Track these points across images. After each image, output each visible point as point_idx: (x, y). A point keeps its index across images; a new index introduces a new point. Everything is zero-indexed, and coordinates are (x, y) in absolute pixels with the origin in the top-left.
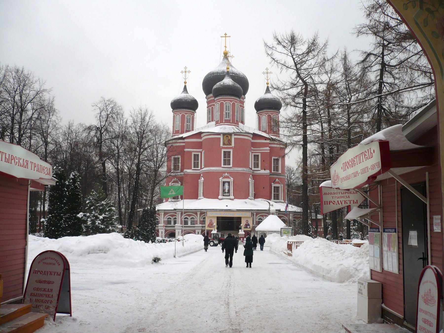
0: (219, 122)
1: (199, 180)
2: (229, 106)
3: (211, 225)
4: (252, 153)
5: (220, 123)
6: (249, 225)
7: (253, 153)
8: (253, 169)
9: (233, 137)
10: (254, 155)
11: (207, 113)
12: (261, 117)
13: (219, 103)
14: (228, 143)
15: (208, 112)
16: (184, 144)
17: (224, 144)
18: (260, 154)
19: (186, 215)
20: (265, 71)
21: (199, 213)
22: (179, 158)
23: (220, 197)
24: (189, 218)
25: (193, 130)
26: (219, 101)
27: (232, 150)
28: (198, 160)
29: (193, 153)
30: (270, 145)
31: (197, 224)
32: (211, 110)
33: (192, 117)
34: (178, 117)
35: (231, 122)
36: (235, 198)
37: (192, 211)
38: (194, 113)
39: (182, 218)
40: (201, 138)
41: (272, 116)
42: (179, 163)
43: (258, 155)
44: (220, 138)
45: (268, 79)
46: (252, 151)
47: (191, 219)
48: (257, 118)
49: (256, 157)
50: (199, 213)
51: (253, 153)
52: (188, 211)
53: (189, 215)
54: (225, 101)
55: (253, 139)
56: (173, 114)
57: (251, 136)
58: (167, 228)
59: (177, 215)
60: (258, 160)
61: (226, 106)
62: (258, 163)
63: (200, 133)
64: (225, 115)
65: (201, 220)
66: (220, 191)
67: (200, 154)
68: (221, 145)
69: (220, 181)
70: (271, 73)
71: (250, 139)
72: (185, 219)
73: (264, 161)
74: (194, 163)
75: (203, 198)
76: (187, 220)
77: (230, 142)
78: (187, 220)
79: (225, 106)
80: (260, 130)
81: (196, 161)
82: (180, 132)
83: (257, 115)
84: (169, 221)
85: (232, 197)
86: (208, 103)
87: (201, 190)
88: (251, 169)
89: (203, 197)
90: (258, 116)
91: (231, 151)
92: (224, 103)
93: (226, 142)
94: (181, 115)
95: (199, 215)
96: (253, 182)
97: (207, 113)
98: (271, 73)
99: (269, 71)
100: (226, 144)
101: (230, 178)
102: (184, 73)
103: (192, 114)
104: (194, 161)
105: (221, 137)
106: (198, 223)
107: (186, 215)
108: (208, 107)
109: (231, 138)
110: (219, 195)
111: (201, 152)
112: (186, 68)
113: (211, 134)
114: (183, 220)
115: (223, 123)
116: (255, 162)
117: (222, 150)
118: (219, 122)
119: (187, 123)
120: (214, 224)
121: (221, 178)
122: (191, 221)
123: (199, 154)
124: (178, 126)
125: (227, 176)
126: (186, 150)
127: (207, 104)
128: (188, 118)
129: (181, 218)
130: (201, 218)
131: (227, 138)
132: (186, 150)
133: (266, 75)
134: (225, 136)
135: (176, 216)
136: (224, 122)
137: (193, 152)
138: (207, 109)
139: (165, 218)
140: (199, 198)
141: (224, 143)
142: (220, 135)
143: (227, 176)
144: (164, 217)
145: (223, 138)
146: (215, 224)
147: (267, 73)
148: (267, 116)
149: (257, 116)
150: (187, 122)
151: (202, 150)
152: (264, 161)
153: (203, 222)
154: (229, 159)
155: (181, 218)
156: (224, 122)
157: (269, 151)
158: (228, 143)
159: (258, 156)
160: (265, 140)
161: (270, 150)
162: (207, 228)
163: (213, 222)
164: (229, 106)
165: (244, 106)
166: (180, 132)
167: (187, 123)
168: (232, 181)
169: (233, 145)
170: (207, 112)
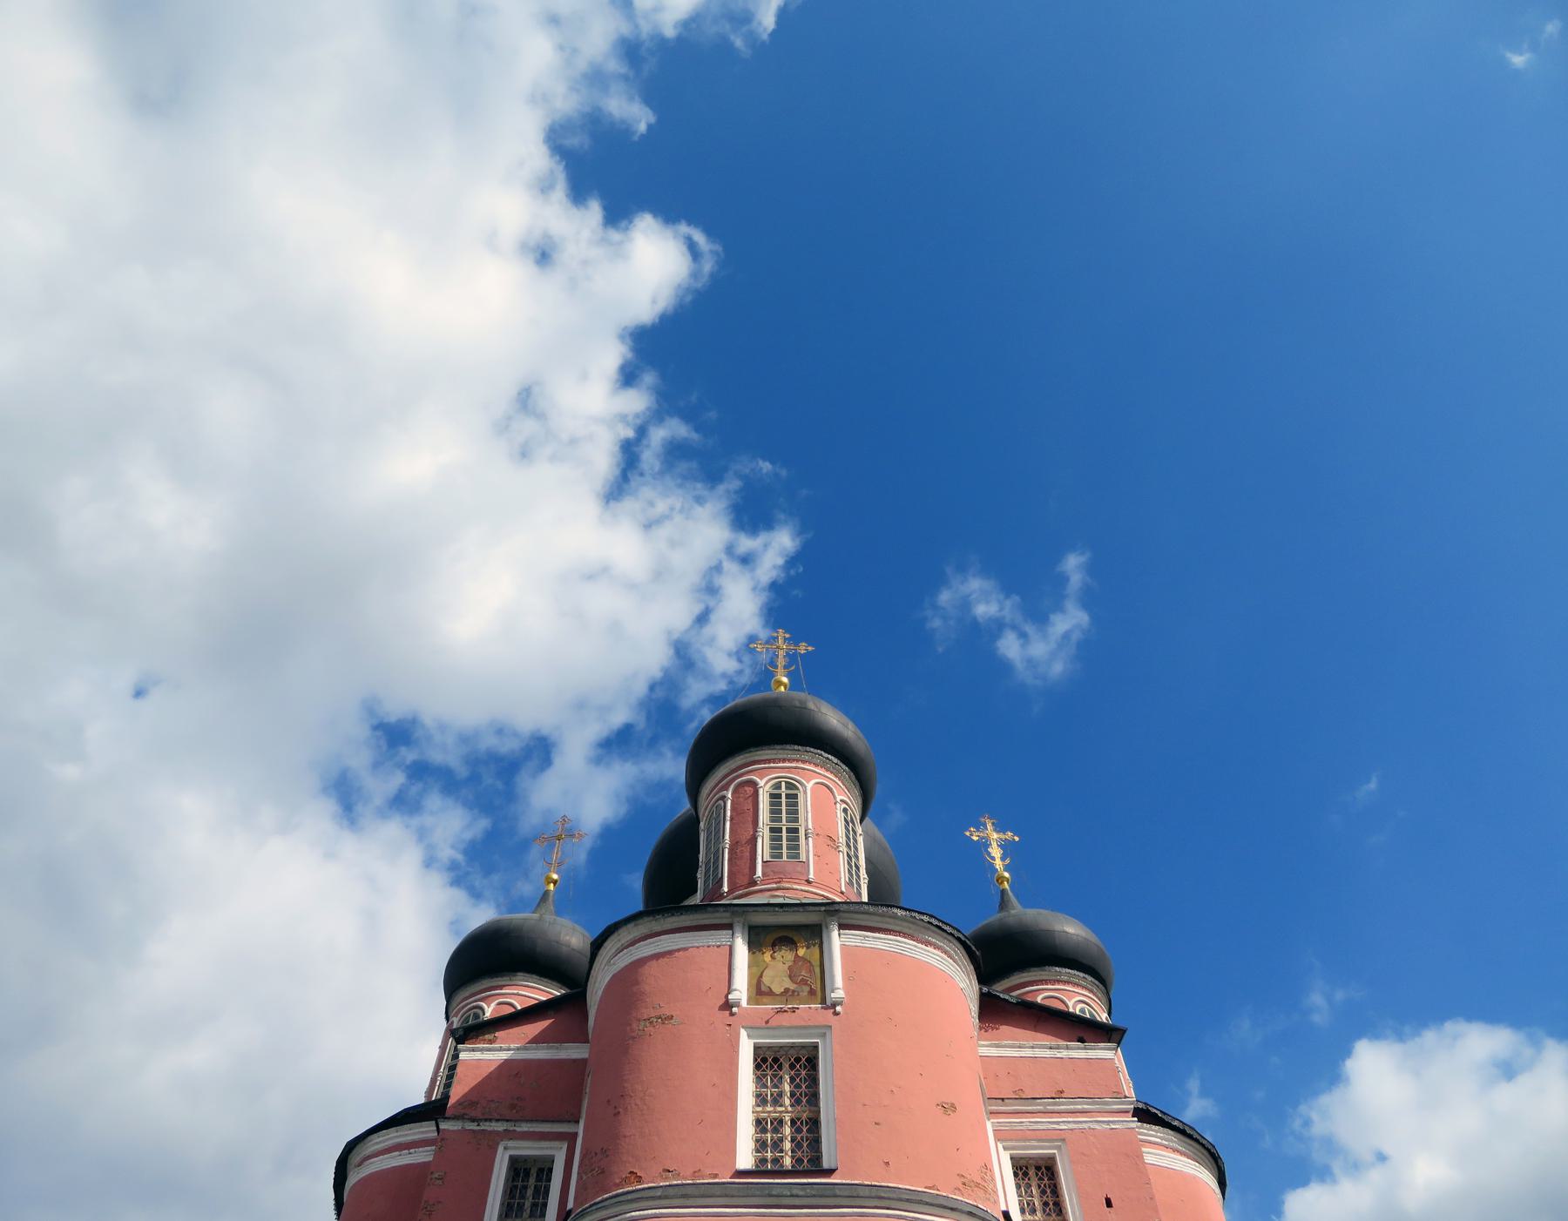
0: (726, 889)
9: (837, 940)
14: (792, 987)
17: (759, 991)
35: (811, 876)
61: (775, 797)
92: (761, 783)
100: (770, 993)
115: (754, 883)
117: (743, 1033)
118: (726, 889)
142: (729, 927)
158: (792, 987)
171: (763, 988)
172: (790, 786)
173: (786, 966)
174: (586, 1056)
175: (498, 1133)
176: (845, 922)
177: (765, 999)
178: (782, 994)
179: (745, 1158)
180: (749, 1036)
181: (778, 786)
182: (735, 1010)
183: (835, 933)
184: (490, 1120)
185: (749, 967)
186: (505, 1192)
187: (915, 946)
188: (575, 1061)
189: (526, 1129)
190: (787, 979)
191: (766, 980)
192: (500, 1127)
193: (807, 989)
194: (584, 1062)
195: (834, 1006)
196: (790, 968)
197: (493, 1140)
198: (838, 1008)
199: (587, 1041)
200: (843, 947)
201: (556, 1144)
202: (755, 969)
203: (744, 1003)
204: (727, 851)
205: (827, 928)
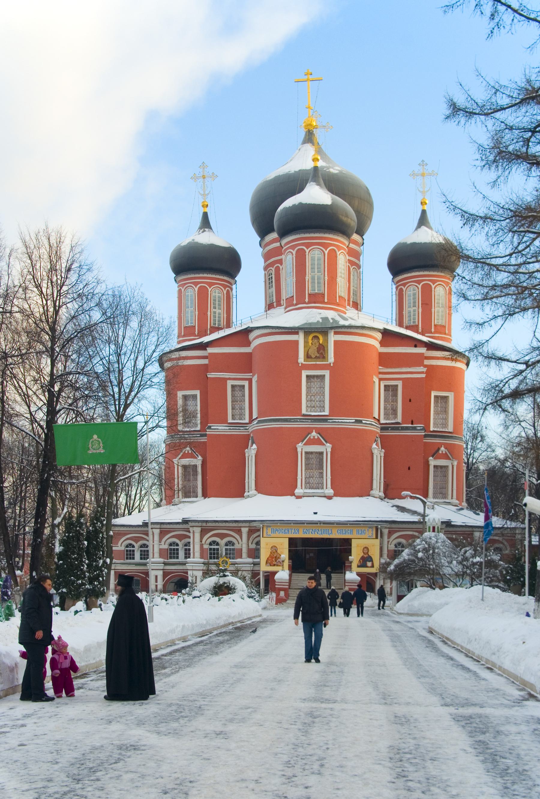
1: (246, 450)
3: (274, 559)
4: (380, 380)
6: (370, 559)
7: (381, 382)
8: (382, 421)
10: (385, 386)
11: (263, 284)
12: (404, 289)
14: (318, 355)
15: (267, 280)
16: (206, 362)
17: (308, 356)
18: (400, 384)
21: (245, 531)
23: (298, 491)
24: (222, 542)
25: (228, 326)
27: (328, 372)
29: (230, 383)
30: (426, 362)
31: (241, 557)
32: (273, 273)
33: (225, 292)
34: (192, 293)
35: (326, 300)
36: (336, 495)
37: (227, 524)
38: (232, 285)
40: (248, 344)
43: (397, 386)
44: (296, 343)
46: (381, 376)
47: (226, 545)
48: (394, 293)
49: (391, 390)
50: (245, 531)
51: (381, 382)
52: (217, 524)
53: (222, 536)
55: (383, 343)
56: (178, 287)
57: (379, 336)
59: (191, 535)
60: (395, 395)
62: (397, 407)
63: (247, 331)
65: (250, 547)
67: (246, 384)
68: (301, 359)
69: (299, 450)
71: (377, 344)
72: (210, 544)
73: (410, 401)
75: (255, 495)
77: (324, 350)
80: (400, 324)
82: (196, 333)
83: (394, 287)
85: (330, 491)
86: (267, 256)
87: (251, 474)
88: (379, 420)
89: (255, 492)
90: (397, 288)
91: (327, 373)
93: (313, 352)
94: (196, 289)
95: (245, 536)
96: (383, 455)
97: (265, 282)
101: (324, 445)
103: (225, 286)
105: (300, 338)
106: (244, 554)
108: (265, 269)
109: (326, 340)
110: (296, 487)
111: (250, 381)
113: (274, 331)
114: (206, 546)
117: (303, 372)
120: (283, 556)
121: (300, 444)
123: (243, 386)
124: (191, 316)
125: (316, 437)
126: (211, 375)
127: (263, 260)
129: (201, 542)
130: (250, 544)
132: (211, 375)
134: (310, 337)
135: (189, 537)
136: (307, 300)
137: (230, 379)
138: (263, 272)
140: (246, 494)
142: (297, 333)
143: (316, 437)
145: (306, 342)
146: (285, 555)
148: (420, 286)
149: (394, 290)
150: (212, 306)
151: (251, 374)
152: (410, 401)
153: (255, 553)
155: (201, 542)
156: (307, 300)
157: (424, 376)
160: (416, 346)
161: (426, 373)
162: (264, 568)
163: (279, 551)
165: (361, 263)
166: (196, 333)
167: (215, 310)
168: (329, 450)
169: (331, 359)
170: (263, 280)
176: (337, 330)
177: (310, 360)
183: (332, 333)
190: (316, 353)
191: (309, 352)
194: (250, 355)
195: (330, 364)
198: (332, 365)
203: (304, 363)
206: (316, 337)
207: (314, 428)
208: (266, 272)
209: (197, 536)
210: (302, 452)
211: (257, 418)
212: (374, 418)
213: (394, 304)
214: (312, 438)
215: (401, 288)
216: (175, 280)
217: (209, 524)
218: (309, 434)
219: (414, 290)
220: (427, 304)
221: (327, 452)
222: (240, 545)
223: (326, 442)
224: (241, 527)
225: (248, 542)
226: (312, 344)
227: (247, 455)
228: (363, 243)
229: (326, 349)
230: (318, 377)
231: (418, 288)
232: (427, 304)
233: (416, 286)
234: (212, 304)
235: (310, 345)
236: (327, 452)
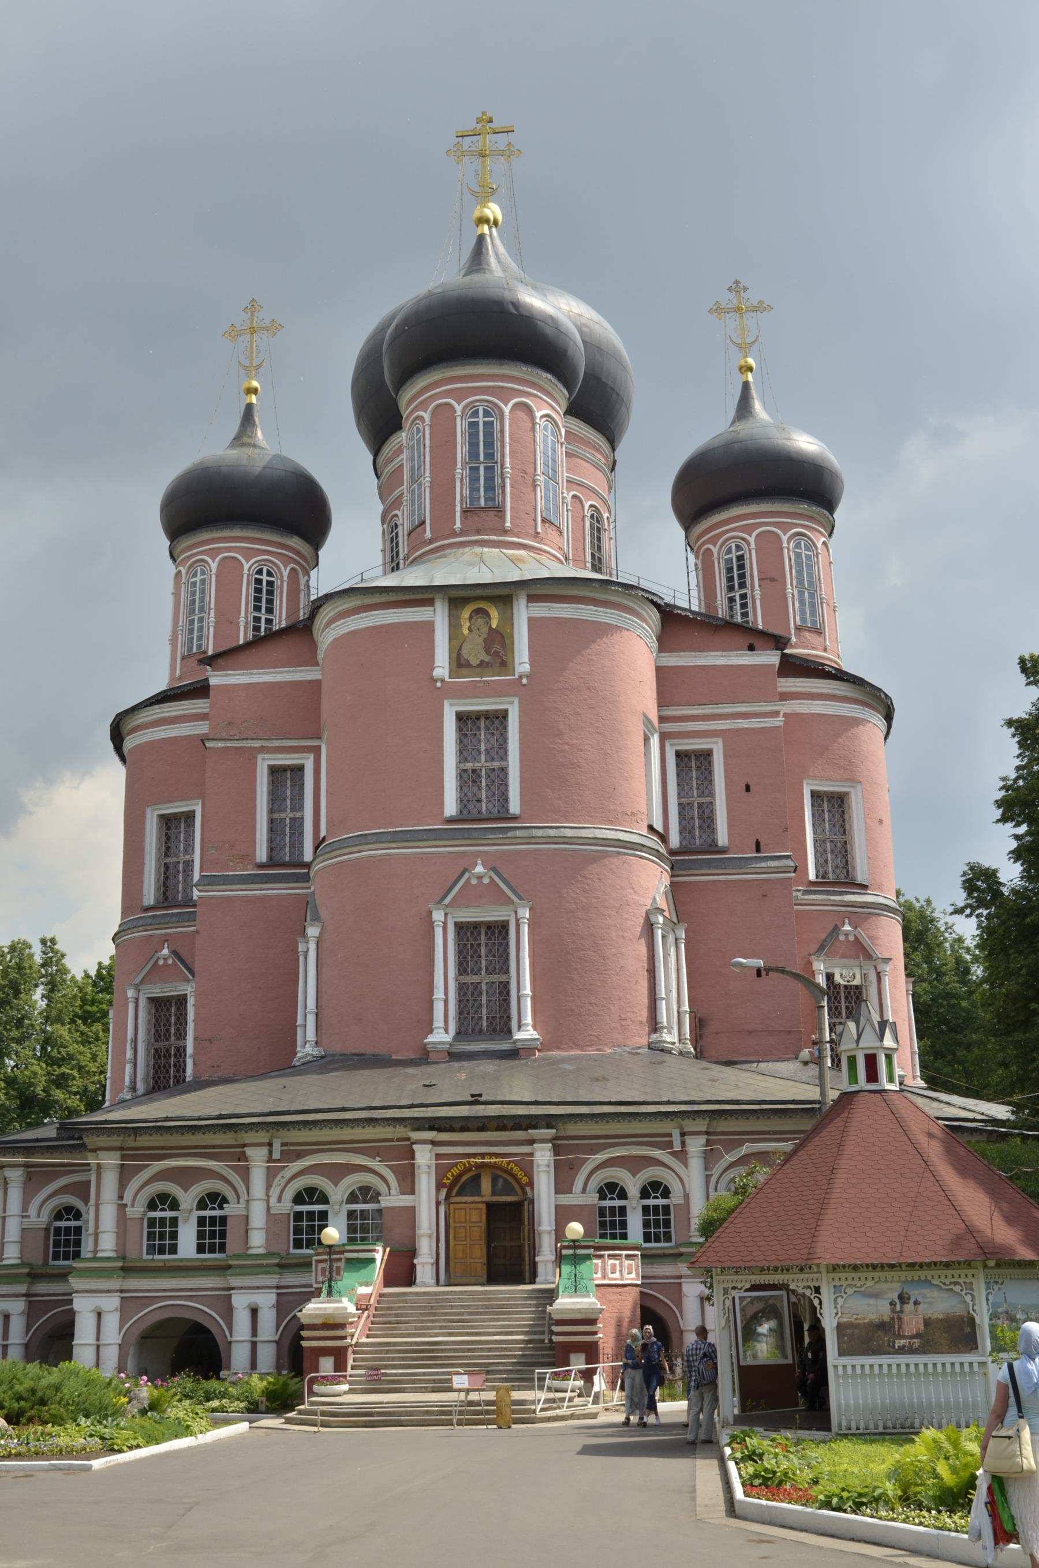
0: (428, 534)
2: (488, 425)
4: (664, 737)
5: (431, 541)
9: (523, 612)
10: (679, 755)
12: (715, 550)
13: (426, 416)
14: (487, 659)
15: (388, 543)
17: (459, 663)
19: (162, 1175)
20: (727, 299)
22: (190, 816)
26: (422, 406)
27: (516, 701)
28: (301, 807)
33: (286, 573)
35: (508, 524)
39: (127, 1199)
41: (785, 538)
42: (189, 848)
45: (749, 340)
47: (202, 1205)
48: (692, 567)
54: (459, 395)
55: (664, 643)
57: (654, 615)
58: (42, 1288)
61: (473, 425)
64: (466, 481)
66: (439, 994)
70: (760, 308)
73: (748, 788)
74: (271, 830)
76: (168, 1214)
78: (168, 1214)
79: (465, 424)
81: (288, 815)
84: (68, 1229)
86: (383, 493)
88: (664, 838)
90: (697, 558)
92: (459, 408)
93: (475, 653)
98: (760, 308)
99: (753, 297)
100: (468, 665)
102: (246, 337)
104: (271, 811)
105: (439, 616)
107: (162, 1175)
109: (508, 619)
111: (316, 751)
112: (252, 307)
114: (137, 1210)
115: (455, 534)
116: (685, 801)
118: (428, 534)
119: (257, 608)
122: (201, 1221)
123: (300, 769)
128: (259, 582)
129: (121, 1198)
130: (273, 1201)
131: (480, 621)
133: (731, 319)
136: (458, 525)
137: (263, 750)
139: (32, 1210)
141: (459, 655)
142: (430, 602)
144: (25, 1208)
145: (454, 627)
147: (738, 310)
148: (752, 540)
152: (748, 788)
154: (496, 764)
155: (121, 1198)
156: (458, 525)
158: (487, 659)
159: (705, 757)
160: (751, 648)
164: (488, 425)
170: (381, 547)
171: (463, 661)
172: (487, 414)
173: (482, 639)
174: (319, 677)
175: (256, 748)
177: (464, 671)
178: (478, 666)
179: (451, 808)
180: (451, 705)
181: (476, 414)
182: (439, 684)
184: (247, 739)
185: (450, 639)
186: (269, 783)
187: (595, 611)
188: (310, 682)
189: (277, 745)
190: (483, 652)
191: (464, 652)
192: (257, 744)
193: (499, 660)
194: (316, 685)
195: (521, 677)
196: (485, 640)
197: (251, 755)
198: (525, 681)
199: (317, 664)
200: (531, 620)
201: (305, 755)
202: (455, 642)
203: (447, 679)
204: (428, 490)
205: (517, 600)
206: (480, 611)
207: (478, 854)
208: (385, 526)
209: (110, 1182)
210: (445, 923)
211: (324, 839)
212: (651, 828)
213: (693, 575)
214: (474, 882)
215: (709, 549)
216: (173, 558)
217: (144, 1141)
218: (465, 871)
219: (738, 548)
220: (772, 580)
221: (517, 920)
222: (242, 1205)
223: (520, 898)
224: (244, 1146)
225: (268, 1195)
226: (470, 629)
227: (301, 947)
228: (615, 462)
229: (507, 641)
230: (488, 716)
231: (748, 544)
232: (772, 580)
233: (743, 539)
234: (251, 598)
235: (466, 631)
236: (517, 920)
